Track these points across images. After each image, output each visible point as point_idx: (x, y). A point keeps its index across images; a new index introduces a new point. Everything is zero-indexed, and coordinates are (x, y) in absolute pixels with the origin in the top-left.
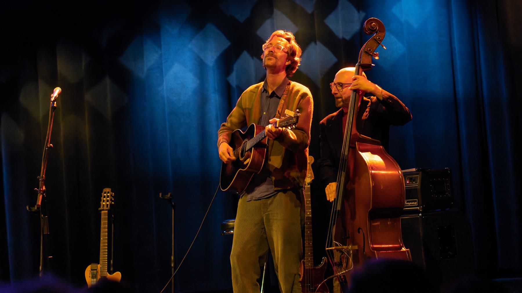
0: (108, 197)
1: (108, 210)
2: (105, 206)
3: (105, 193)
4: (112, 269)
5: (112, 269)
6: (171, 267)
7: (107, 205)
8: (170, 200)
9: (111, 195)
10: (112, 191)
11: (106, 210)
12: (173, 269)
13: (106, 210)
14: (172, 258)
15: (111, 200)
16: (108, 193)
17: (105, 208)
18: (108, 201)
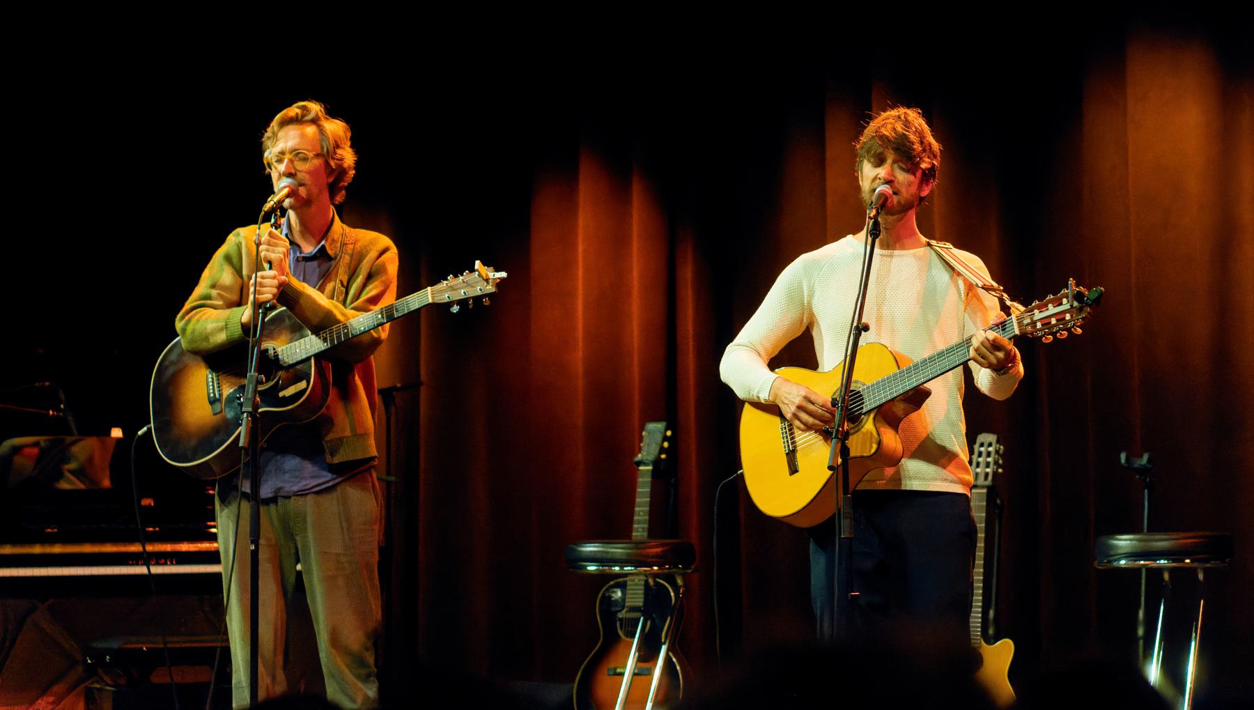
0: (989, 454)
1: (988, 487)
2: (982, 477)
3: (982, 445)
4: (991, 632)
5: (991, 632)
6: (1136, 639)
7: (987, 475)
8: (1142, 471)
9: (997, 452)
10: (998, 442)
11: (983, 487)
12: (1141, 642)
13: (983, 487)
14: (1141, 614)
15: (996, 463)
16: (990, 445)
17: (981, 481)
18: (988, 465)
